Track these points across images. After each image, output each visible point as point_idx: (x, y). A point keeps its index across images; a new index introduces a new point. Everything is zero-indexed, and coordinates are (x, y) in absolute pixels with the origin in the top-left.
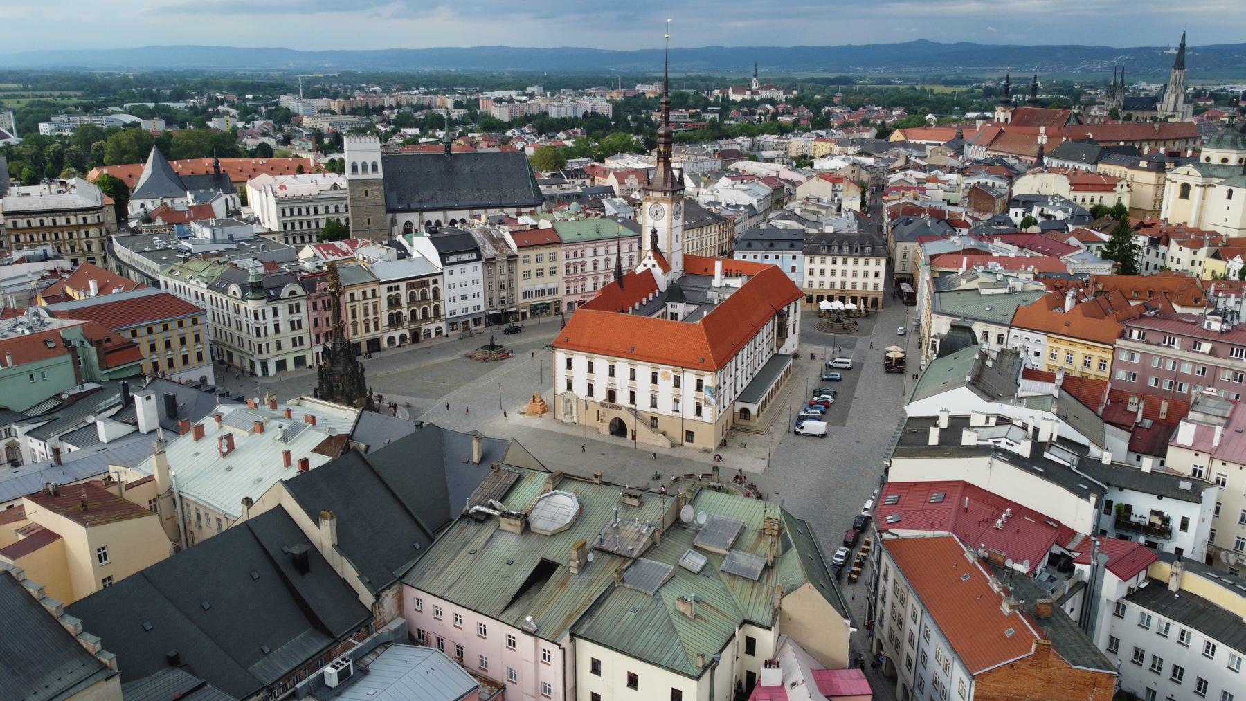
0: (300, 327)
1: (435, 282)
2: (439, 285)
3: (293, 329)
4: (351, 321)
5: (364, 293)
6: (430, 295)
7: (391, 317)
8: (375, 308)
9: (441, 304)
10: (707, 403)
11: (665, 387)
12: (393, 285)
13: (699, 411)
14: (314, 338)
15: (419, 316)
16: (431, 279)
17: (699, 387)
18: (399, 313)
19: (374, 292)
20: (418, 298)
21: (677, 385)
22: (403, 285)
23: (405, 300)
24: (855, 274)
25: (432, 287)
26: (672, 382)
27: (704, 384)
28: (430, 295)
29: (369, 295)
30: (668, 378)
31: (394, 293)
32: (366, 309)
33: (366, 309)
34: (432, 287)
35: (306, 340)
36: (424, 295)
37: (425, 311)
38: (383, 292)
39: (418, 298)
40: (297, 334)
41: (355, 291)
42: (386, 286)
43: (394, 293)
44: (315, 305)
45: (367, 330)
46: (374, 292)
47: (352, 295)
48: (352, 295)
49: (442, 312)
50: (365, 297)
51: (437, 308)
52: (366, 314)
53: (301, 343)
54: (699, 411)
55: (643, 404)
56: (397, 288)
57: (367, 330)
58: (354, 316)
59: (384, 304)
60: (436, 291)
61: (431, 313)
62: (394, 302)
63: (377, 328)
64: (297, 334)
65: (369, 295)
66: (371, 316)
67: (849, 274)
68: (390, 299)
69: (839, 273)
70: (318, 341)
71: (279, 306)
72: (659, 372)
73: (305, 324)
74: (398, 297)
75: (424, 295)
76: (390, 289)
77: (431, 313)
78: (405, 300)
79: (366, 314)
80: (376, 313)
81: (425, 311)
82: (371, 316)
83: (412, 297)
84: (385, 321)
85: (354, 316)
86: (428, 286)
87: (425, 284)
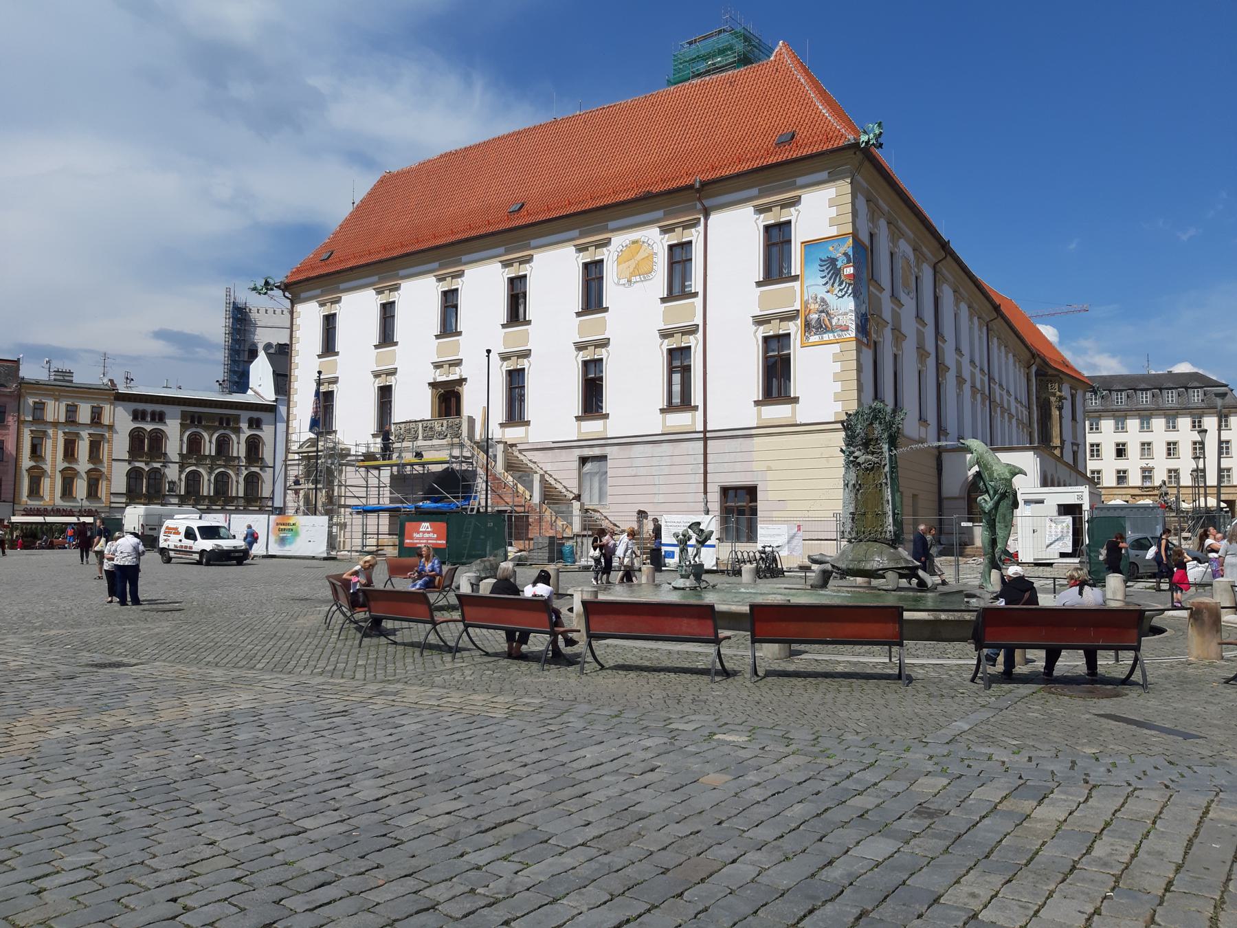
1: (255, 424)
2: (266, 433)
4: (26, 462)
5: (72, 410)
6: (239, 448)
7: (134, 476)
9: (267, 475)
10: (817, 326)
11: (637, 314)
12: (149, 408)
13: (776, 375)
15: (207, 488)
16: (245, 415)
17: (776, 267)
18: (156, 476)
20: (209, 448)
21: (678, 288)
23: (174, 445)
24: (1172, 448)
26: (659, 282)
27: (799, 236)
28: (239, 448)
30: (642, 271)
31: (149, 427)
34: (246, 432)
36: (223, 444)
37: (222, 482)
39: (209, 448)
45: (67, 492)
47: (39, 407)
49: (266, 492)
51: (252, 481)
54: (776, 375)
56: (160, 417)
57: (67, 492)
59: (119, 445)
60: (254, 446)
61: (238, 488)
62: (145, 445)
63: (92, 493)
66: (83, 464)
67: (1160, 450)
68: (136, 438)
69: (1133, 450)
72: (609, 256)
74: (158, 439)
75: (223, 444)
77: (238, 488)
78: (174, 445)
81: (222, 482)
82: (83, 464)
83: (194, 444)
84: (118, 479)
86: (238, 431)
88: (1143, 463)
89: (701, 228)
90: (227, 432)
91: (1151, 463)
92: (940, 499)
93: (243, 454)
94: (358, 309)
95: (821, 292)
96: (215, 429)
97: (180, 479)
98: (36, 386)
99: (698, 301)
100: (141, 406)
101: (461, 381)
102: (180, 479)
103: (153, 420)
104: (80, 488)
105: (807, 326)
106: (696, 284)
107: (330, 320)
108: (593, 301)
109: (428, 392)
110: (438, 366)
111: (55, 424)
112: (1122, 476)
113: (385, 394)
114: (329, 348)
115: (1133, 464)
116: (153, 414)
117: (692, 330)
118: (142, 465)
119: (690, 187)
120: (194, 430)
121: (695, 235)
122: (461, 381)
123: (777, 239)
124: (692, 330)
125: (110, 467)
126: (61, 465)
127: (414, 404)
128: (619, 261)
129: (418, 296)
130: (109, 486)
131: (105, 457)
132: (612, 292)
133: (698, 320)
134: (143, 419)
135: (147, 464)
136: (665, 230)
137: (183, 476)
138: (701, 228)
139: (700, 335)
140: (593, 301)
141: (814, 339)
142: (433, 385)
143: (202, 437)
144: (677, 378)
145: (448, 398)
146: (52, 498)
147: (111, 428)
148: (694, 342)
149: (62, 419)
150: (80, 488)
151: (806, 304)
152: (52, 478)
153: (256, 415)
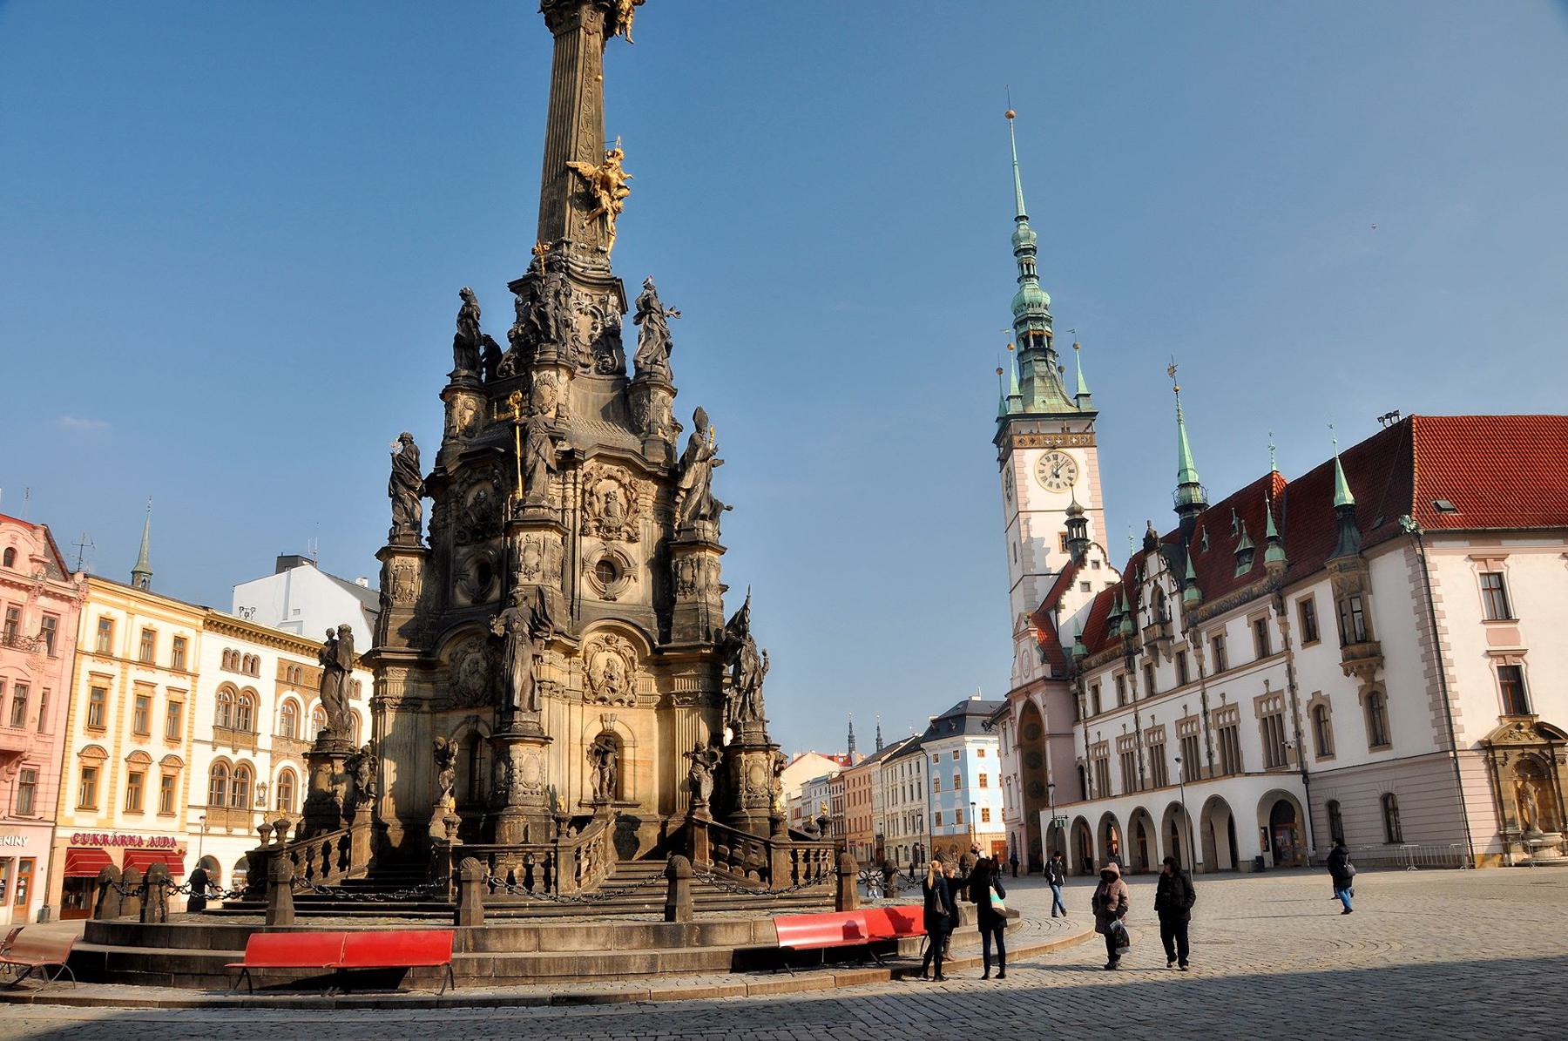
12: (244, 647)
18: (245, 770)
29: (164, 654)
31: (241, 681)
32: (143, 702)
33: (143, 702)
41: (119, 615)
47: (106, 625)
48: (106, 625)
50: (147, 662)
52: (142, 732)
56: (252, 665)
59: (203, 715)
65: (164, 654)
76: (230, 659)
79: (142, 732)
80: (173, 738)
97: (271, 782)
102: (271, 782)
126: (129, 746)
130: (185, 793)
131: (184, 734)
135: (235, 752)
147: (195, 676)
149: (135, 657)
152: (115, 767)
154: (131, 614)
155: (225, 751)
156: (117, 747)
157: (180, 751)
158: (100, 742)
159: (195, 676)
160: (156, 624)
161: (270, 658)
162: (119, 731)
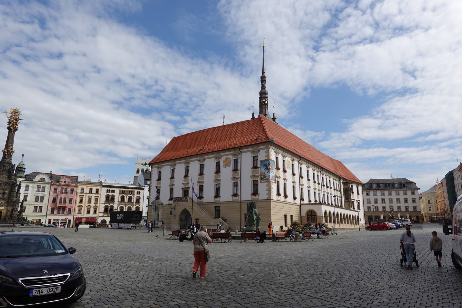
0: (42, 201)
1: (139, 193)
2: (141, 196)
3: (37, 200)
4: (78, 204)
6: (134, 200)
8: (96, 199)
12: (111, 189)
14: (50, 209)
16: (136, 191)
18: (112, 207)
19: (97, 190)
20: (126, 200)
22: (117, 191)
23: (117, 199)
25: (136, 195)
26: (232, 167)
28: (134, 200)
29: (94, 191)
30: (228, 164)
31: (110, 194)
32: (90, 200)
33: (90, 200)
34: (136, 195)
35: (44, 210)
36: (130, 200)
38: (103, 192)
39: (126, 200)
40: (39, 204)
41: (85, 187)
42: (106, 189)
43: (110, 194)
44: (56, 189)
45: (88, 212)
46: (97, 190)
47: (83, 189)
48: (83, 189)
53: (41, 211)
55: (209, 196)
56: (113, 191)
57: (88, 212)
58: (81, 201)
59: (102, 199)
63: (95, 212)
64: (39, 204)
65: (94, 191)
66: (92, 204)
67: (395, 201)
69: (387, 201)
70: (52, 212)
71: (31, 185)
72: (221, 160)
73: (46, 199)
74: (113, 197)
75: (130, 200)
76: (108, 191)
78: (117, 199)
82: (92, 204)
83: (122, 199)
85: (81, 201)
87: (131, 193)
88: (390, 205)
89: (240, 155)
90: (131, 195)
91: (392, 205)
92: (301, 216)
93: (135, 201)
94: (166, 170)
95: (264, 172)
96: (128, 194)
98: (82, 183)
99: (239, 172)
100: (109, 189)
101: (189, 188)
103: (112, 192)
104: (92, 210)
105: (261, 178)
106: (239, 168)
107: (160, 173)
108: (218, 172)
109: (181, 190)
110: (183, 184)
111: (86, 193)
112: (384, 208)
113: (172, 190)
114: (159, 179)
115: (387, 205)
116: (112, 190)
117: (238, 178)
118: (108, 204)
119: (237, 147)
120: (122, 195)
121: (239, 157)
122: (189, 188)
123: (255, 159)
124: (238, 178)
125: (99, 205)
126: (87, 205)
127: (178, 193)
128: (223, 162)
129: (180, 168)
132: (222, 169)
133: (240, 176)
134: (109, 192)
136: (233, 155)
137: (119, 207)
138: (240, 155)
139: (240, 179)
140: (218, 172)
141: (263, 181)
142: (182, 188)
143: (124, 197)
144: (235, 188)
145: (186, 192)
146: (84, 214)
147: (100, 194)
148: (239, 181)
149: (88, 192)
150: (92, 210)
151: (261, 174)
153: (139, 191)
154: (87, 187)
155: (106, 204)
156: (85, 205)
157: (98, 205)
158: (90, 205)
159: (100, 194)
160: (92, 188)
161: (117, 191)
162: (85, 202)
